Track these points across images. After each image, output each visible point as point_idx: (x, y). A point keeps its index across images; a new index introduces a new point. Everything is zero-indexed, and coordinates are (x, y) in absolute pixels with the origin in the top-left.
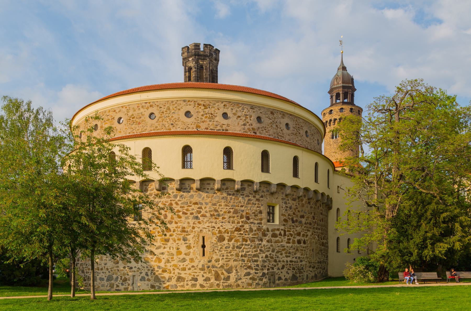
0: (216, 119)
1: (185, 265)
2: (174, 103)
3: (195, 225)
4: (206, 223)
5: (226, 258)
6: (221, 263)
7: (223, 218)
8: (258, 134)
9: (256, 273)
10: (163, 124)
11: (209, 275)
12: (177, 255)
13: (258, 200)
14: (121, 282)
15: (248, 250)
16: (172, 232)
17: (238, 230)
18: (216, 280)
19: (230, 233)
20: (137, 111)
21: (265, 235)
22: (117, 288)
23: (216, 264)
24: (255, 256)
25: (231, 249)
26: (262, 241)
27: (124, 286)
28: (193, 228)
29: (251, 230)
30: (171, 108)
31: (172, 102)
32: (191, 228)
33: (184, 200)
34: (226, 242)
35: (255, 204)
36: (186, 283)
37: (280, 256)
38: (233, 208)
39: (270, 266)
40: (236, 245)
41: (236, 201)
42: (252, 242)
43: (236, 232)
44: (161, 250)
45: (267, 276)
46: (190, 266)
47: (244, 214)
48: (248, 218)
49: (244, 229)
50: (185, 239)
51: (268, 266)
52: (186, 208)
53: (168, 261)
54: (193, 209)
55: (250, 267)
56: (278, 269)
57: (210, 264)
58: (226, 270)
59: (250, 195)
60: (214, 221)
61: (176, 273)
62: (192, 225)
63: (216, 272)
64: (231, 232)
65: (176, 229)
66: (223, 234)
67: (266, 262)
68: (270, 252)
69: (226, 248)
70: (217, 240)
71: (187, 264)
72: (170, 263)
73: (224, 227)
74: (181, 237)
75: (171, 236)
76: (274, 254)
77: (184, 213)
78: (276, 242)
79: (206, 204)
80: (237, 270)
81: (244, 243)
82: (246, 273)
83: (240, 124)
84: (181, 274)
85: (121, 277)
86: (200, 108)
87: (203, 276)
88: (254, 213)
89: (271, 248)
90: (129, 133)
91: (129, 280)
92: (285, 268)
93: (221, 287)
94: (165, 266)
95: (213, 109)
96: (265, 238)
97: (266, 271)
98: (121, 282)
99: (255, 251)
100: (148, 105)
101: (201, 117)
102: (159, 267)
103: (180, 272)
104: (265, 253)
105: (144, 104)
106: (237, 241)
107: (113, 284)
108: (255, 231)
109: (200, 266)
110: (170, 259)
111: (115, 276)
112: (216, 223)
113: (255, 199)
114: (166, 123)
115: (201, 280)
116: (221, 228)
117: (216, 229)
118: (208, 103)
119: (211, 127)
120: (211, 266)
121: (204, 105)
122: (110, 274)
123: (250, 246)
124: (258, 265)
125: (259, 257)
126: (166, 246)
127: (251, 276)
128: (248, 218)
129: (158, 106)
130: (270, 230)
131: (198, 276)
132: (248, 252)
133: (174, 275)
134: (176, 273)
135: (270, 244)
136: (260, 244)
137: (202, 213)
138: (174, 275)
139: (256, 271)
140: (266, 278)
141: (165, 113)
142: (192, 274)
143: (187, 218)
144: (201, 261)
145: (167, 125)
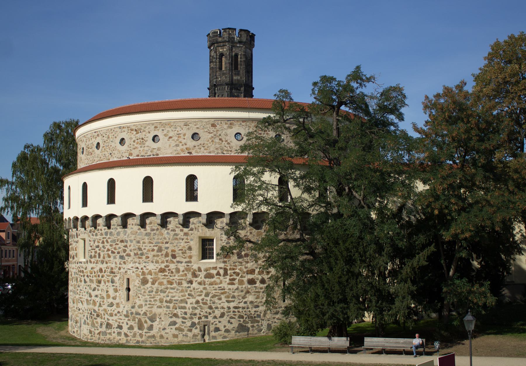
0: (147, 144)
3: (121, 266)
4: (130, 263)
5: (149, 304)
6: (144, 309)
8: (194, 154)
9: (183, 322)
11: (131, 323)
13: (186, 234)
15: (174, 294)
17: (162, 270)
18: (139, 329)
19: (153, 274)
21: (195, 275)
23: (139, 310)
24: (182, 301)
25: (154, 293)
26: (192, 284)
28: (120, 269)
29: (178, 271)
30: (110, 137)
32: (117, 269)
34: (149, 285)
35: (183, 239)
36: (113, 330)
37: (217, 301)
38: (156, 246)
39: (202, 313)
40: (160, 289)
41: (160, 237)
42: (179, 284)
43: (160, 274)
44: (96, 293)
45: (198, 327)
46: (116, 312)
47: (169, 251)
49: (169, 270)
51: (200, 314)
52: (114, 246)
54: (120, 248)
55: (176, 315)
56: (215, 317)
57: (134, 310)
58: (149, 318)
59: (177, 229)
60: (137, 260)
61: (106, 319)
62: (118, 266)
63: (140, 320)
64: (155, 273)
66: (146, 276)
67: (196, 308)
68: (203, 297)
69: (149, 292)
70: (140, 283)
73: (147, 267)
74: (110, 278)
75: (102, 277)
76: (208, 298)
77: (113, 252)
78: (211, 284)
79: (131, 241)
80: (160, 318)
81: (169, 286)
82: (171, 322)
83: (172, 146)
87: (127, 324)
88: (182, 250)
89: (204, 291)
92: (225, 317)
93: (144, 338)
95: (144, 133)
96: (196, 279)
97: (196, 320)
99: (182, 296)
100: (96, 134)
102: (94, 311)
104: (195, 298)
106: (161, 284)
108: (183, 271)
109: (125, 313)
112: (139, 263)
113: (182, 234)
115: (125, 329)
116: (144, 269)
117: (140, 270)
118: (139, 127)
119: (142, 154)
120: (134, 312)
121: (136, 130)
123: (175, 290)
124: (186, 313)
127: (177, 326)
128: (174, 256)
130: (202, 269)
131: (123, 323)
132: (174, 297)
135: (201, 287)
136: (189, 287)
137: (127, 252)
139: (184, 320)
140: (196, 328)
142: (118, 320)
143: (115, 258)
144: (125, 307)
145: (107, 156)
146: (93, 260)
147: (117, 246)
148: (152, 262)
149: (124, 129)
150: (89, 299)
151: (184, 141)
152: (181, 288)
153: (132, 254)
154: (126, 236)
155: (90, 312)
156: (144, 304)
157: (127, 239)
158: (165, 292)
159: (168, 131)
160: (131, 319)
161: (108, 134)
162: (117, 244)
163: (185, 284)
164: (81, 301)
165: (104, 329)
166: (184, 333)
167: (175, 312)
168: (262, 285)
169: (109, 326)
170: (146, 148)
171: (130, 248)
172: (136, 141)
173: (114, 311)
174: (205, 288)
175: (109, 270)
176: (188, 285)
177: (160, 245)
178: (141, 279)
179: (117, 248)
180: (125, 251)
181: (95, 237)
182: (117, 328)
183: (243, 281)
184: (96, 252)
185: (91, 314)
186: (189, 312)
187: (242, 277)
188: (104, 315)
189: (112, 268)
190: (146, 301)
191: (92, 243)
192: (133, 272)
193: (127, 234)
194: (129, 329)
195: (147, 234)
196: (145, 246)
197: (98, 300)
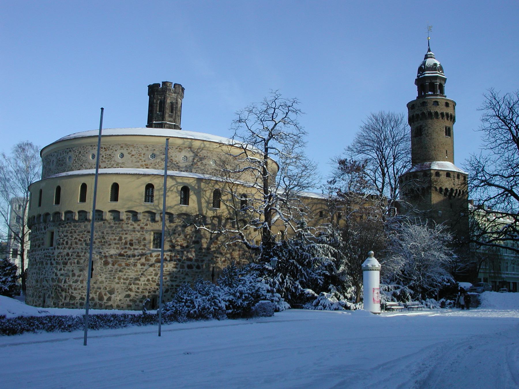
6: (104, 285)
9: (136, 295)
23: (101, 285)
30: (82, 152)
32: (83, 253)
44: (62, 272)
46: (80, 287)
48: (131, 244)
55: (130, 290)
58: (108, 292)
63: (100, 293)
69: (110, 271)
74: (76, 261)
77: (80, 240)
89: (154, 272)
92: (169, 293)
94: (64, 286)
100: (68, 150)
121: (105, 148)
125: (140, 280)
127: (131, 298)
128: (131, 244)
134: (70, 293)
146: (60, 247)
150: (55, 277)
151: (143, 159)
152: (136, 269)
155: (55, 288)
158: (122, 272)
159: (132, 151)
161: (80, 150)
162: (84, 234)
163: (139, 265)
164: (46, 280)
165: (68, 300)
166: (136, 304)
168: (197, 270)
170: (113, 162)
174: (154, 270)
176: (141, 267)
177: (121, 235)
181: (64, 229)
183: (183, 266)
184: (64, 241)
186: (141, 287)
187: (183, 263)
188: (69, 289)
189: (78, 253)
190: (107, 279)
191: (61, 233)
197: (62, 277)
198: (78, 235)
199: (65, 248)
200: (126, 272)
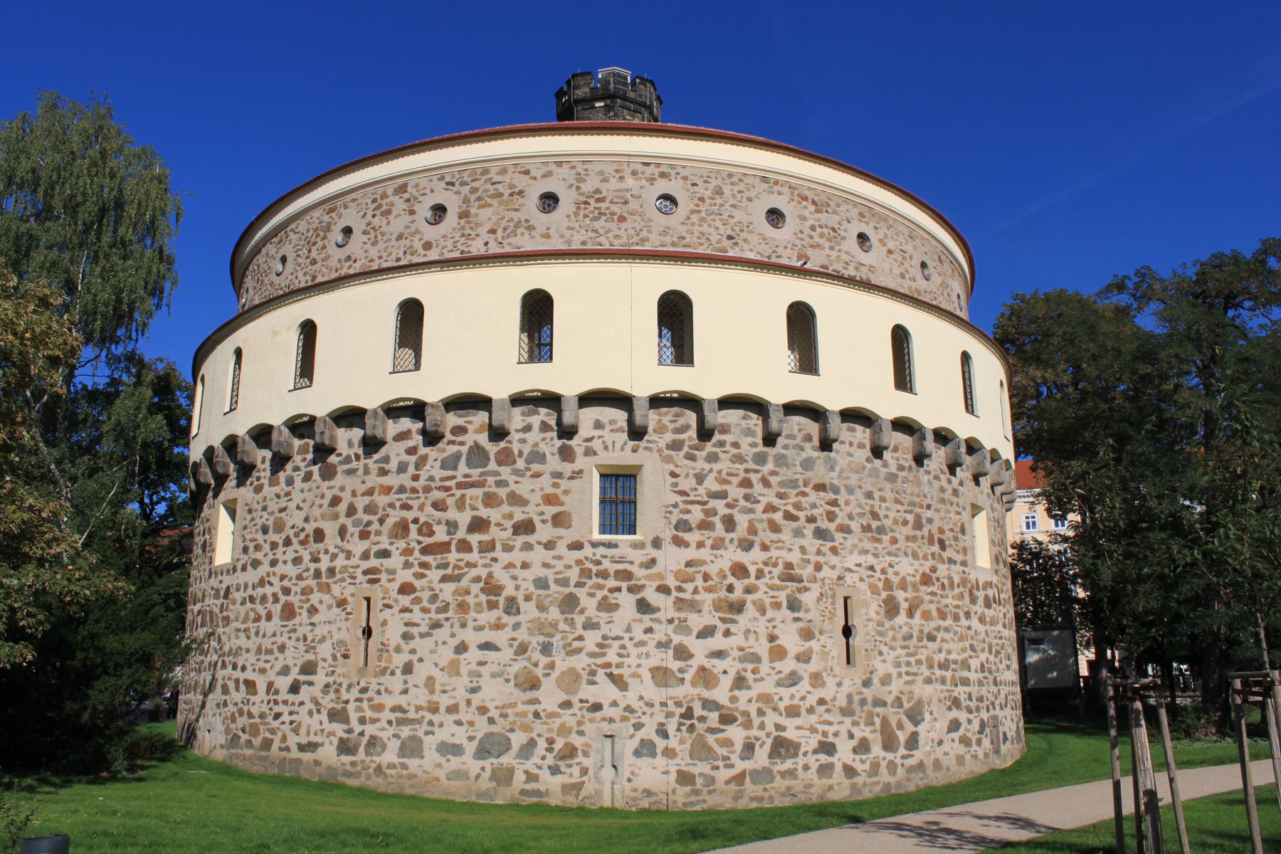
1: (798, 696)
2: (735, 179)
3: (821, 559)
4: (851, 552)
5: (908, 673)
6: (896, 687)
7: (894, 541)
10: (703, 234)
12: (772, 661)
14: (550, 760)
15: (950, 646)
16: (752, 580)
19: (910, 588)
20: (614, 184)
22: (529, 787)
27: (559, 779)
28: (818, 567)
31: (730, 175)
32: (810, 568)
33: (785, 474)
34: (902, 618)
36: (801, 760)
38: (911, 512)
40: (926, 630)
43: (923, 588)
44: (717, 642)
46: (812, 700)
50: (794, 605)
52: (793, 499)
53: (740, 682)
54: (814, 506)
55: (956, 703)
57: (868, 693)
58: (907, 714)
60: (868, 545)
61: (770, 727)
62: (813, 558)
63: (885, 722)
64: (914, 586)
65: (766, 569)
69: (905, 639)
70: (882, 611)
71: (803, 693)
72: (749, 688)
74: (782, 597)
75: (748, 591)
77: (789, 517)
84: (783, 729)
85: (551, 741)
86: (806, 207)
87: (851, 736)
90: (584, 243)
91: (586, 754)
94: (734, 699)
98: (550, 760)
101: (807, 231)
102: (709, 705)
103: (783, 721)
105: (640, 168)
107: (510, 772)
109: (842, 702)
110: (749, 676)
111: (518, 739)
112: (876, 556)
114: (712, 230)
115: (845, 752)
116: (890, 571)
117: (878, 574)
121: (814, 203)
122: (494, 729)
123: (951, 635)
126: (733, 628)
129: (685, 178)
131: (836, 734)
133: (762, 734)
134: (770, 727)
137: (838, 521)
138: (762, 734)
141: (708, 201)
142: (821, 728)
143: (798, 533)
145: (714, 238)
146: (693, 537)
147: (803, 500)
148: (906, 554)
149: (776, 188)
150: (675, 665)
153: (855, 526)
154: (834, 474)
156: (894, 672)
157: (835, 482)
160: (862, 721)
162: (804, 494)
167: (956, 694)
169: (782, 748)
171: (848, 509)
172: (819, 230)
173: (803, 698)
175: (777, 571)
177: (917, 510)
178: (884, 601)
179: (805, 505)
180: (831, 517)
182: (815, 752)
185: (688, 714)
189: (789, 566)
192: (861, 580)
193: (838, 469)
194: (855, 751)
195: (892, 478)
196: (888, 509)
198: (781, 496)
199: (718, 545)
200: (943, 640)
